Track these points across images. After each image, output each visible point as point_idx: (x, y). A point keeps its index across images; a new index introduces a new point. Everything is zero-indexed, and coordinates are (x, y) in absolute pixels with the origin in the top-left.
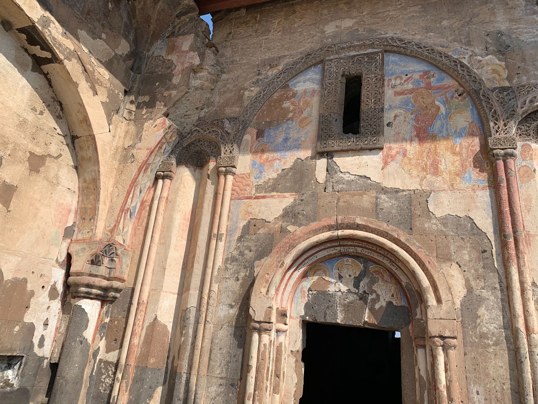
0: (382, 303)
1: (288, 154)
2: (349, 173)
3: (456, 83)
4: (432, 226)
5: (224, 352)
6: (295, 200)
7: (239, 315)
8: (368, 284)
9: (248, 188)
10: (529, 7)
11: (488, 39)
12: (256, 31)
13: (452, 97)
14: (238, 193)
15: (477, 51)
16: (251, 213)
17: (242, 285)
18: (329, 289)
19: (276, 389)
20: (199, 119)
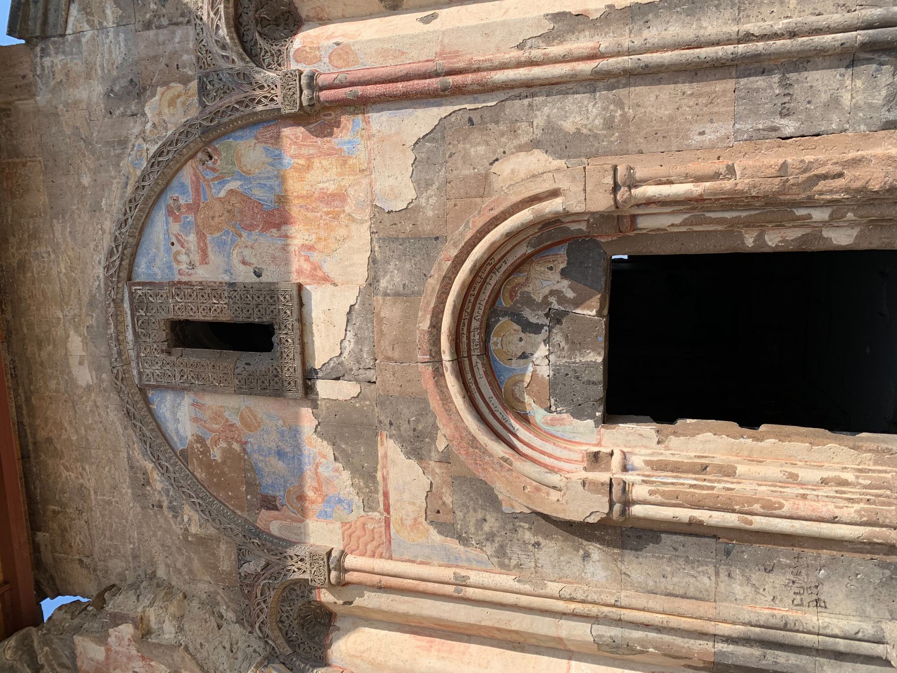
0: (564, 286)
1: (307, 450)
2: (342, 342)
3: (189, 163)
4: (430, 205)
5: (669, 569)
6: (391, 437)
7: (601, 541)
8: (533, 310)
9: (370, 526)
10: (67, 49)
11: (118, 112)
12: (80, 512)
13: (214, 170)
14: (379, 545)
15: (136, 130)
16: (415, 519)
17: (546, 536)
18: (545, 376)
19: (728, 472)
20: (240, 621)
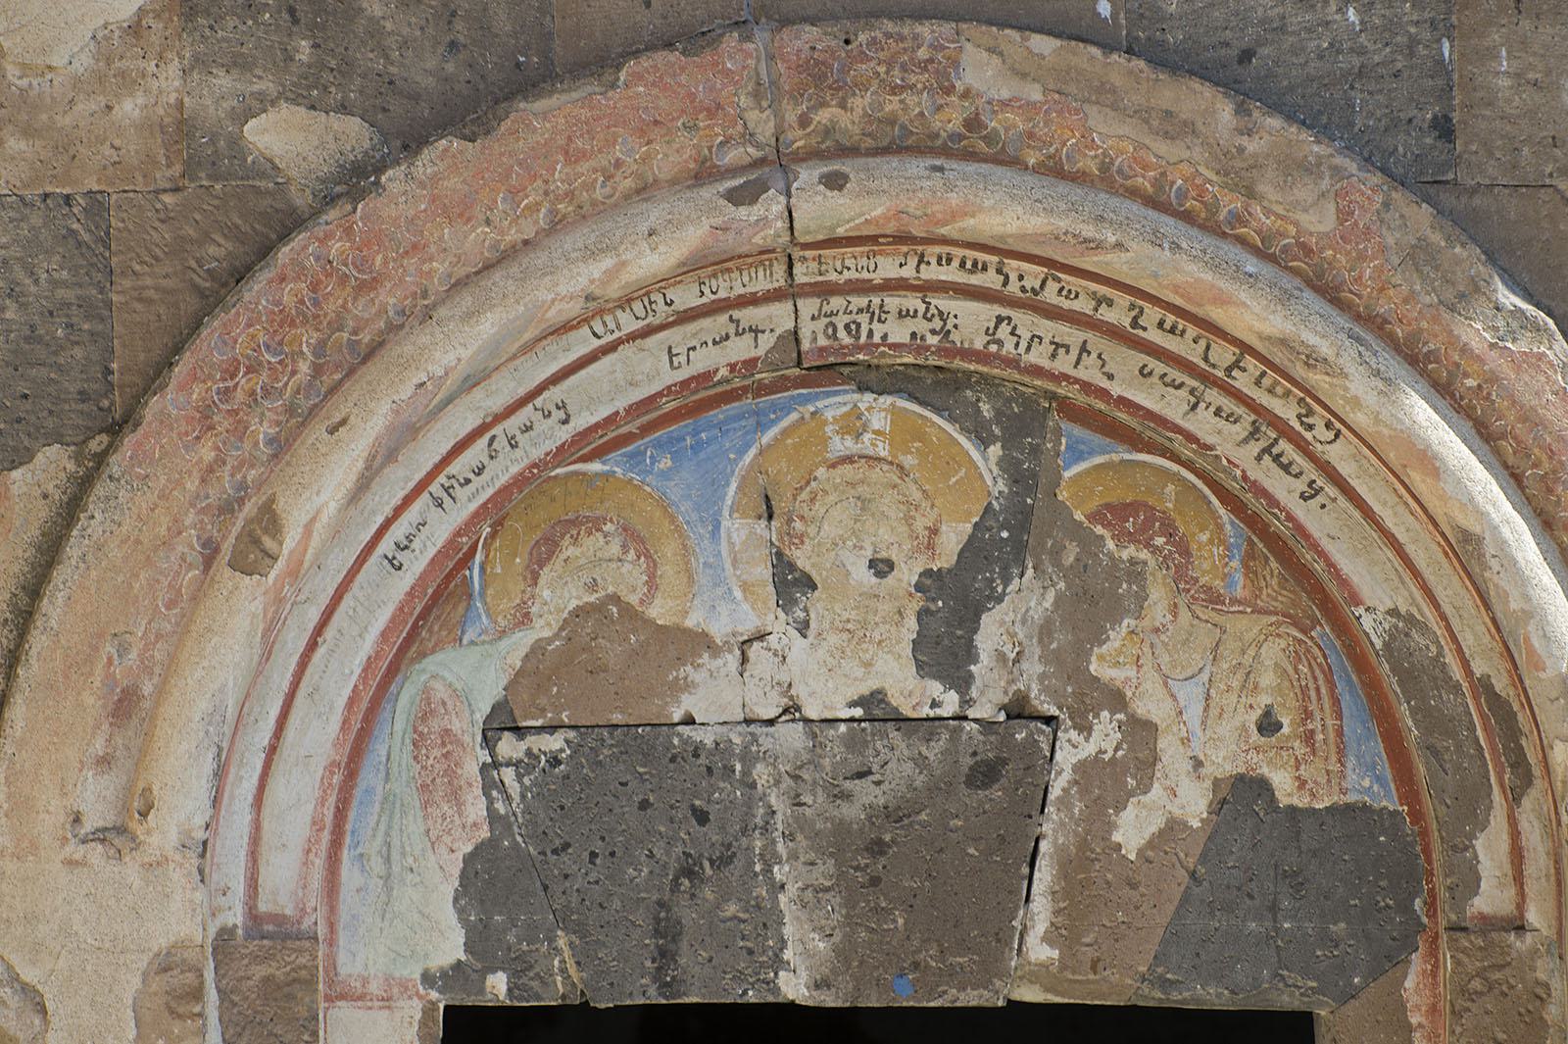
8: (1045, 632)
18: (687, 704)
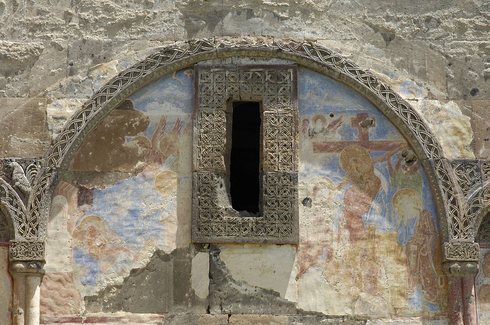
2: (245, 282)
3: (405, 142)
9: (71, 302)
13: (398, 166)
